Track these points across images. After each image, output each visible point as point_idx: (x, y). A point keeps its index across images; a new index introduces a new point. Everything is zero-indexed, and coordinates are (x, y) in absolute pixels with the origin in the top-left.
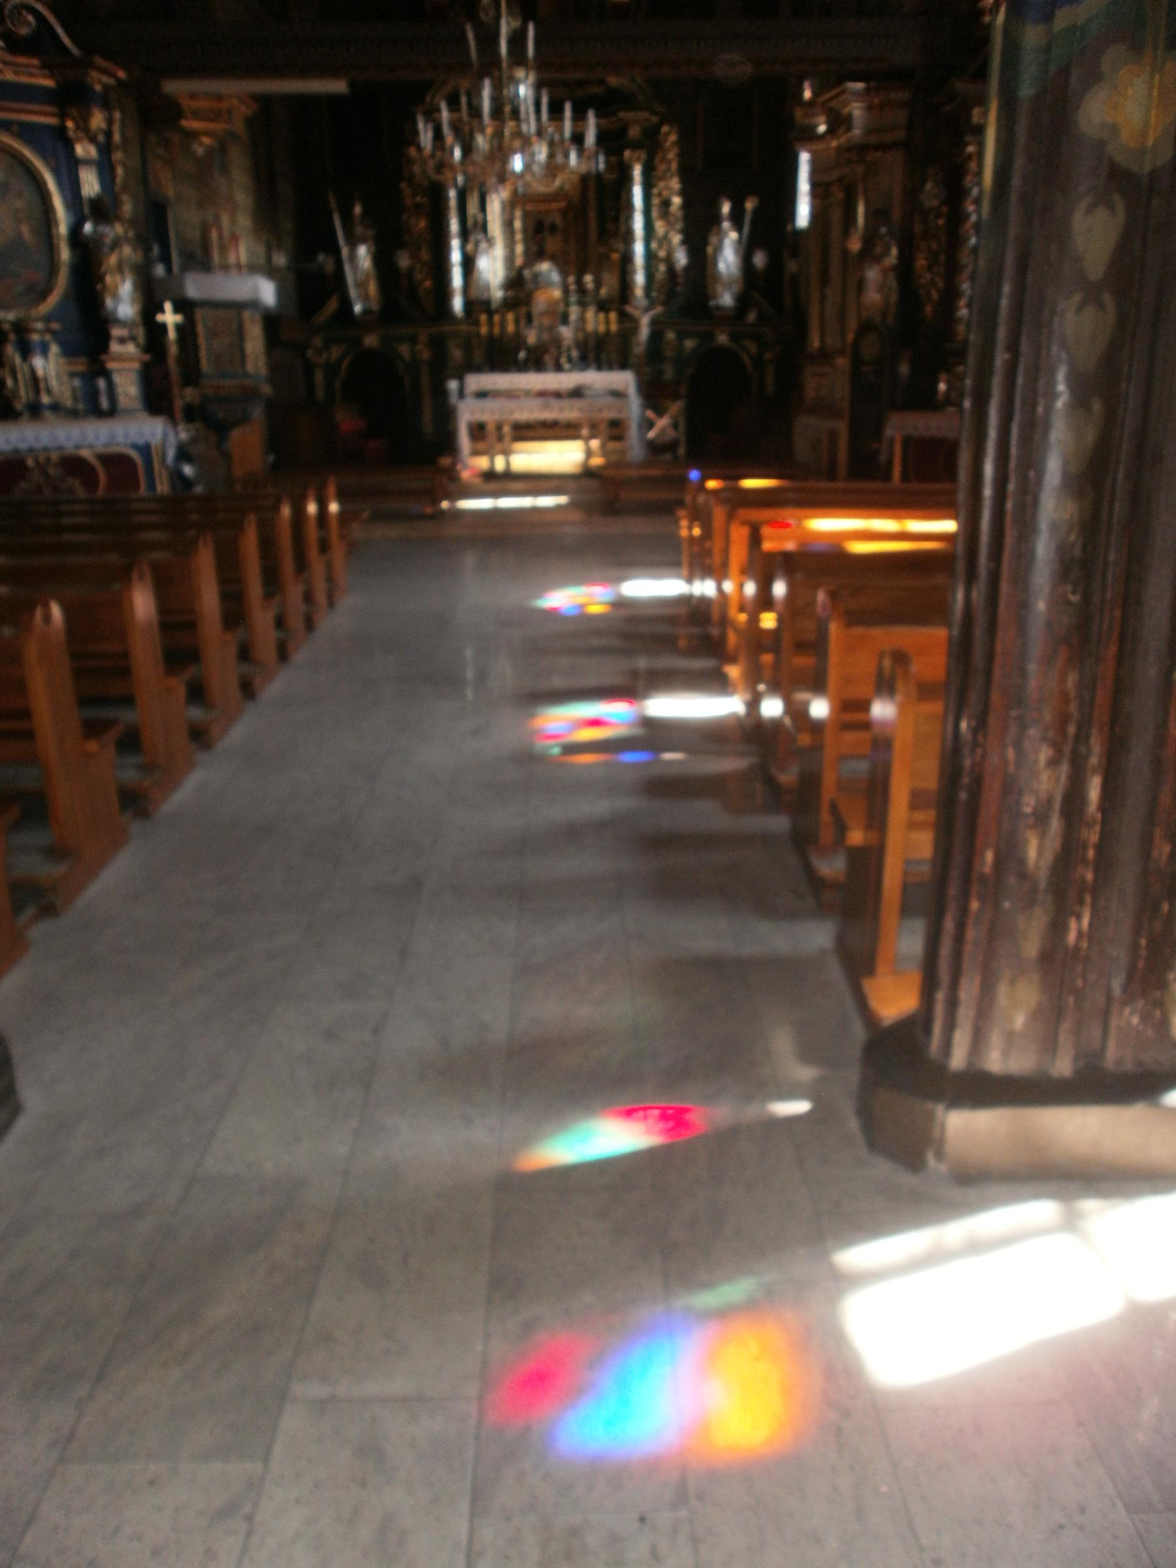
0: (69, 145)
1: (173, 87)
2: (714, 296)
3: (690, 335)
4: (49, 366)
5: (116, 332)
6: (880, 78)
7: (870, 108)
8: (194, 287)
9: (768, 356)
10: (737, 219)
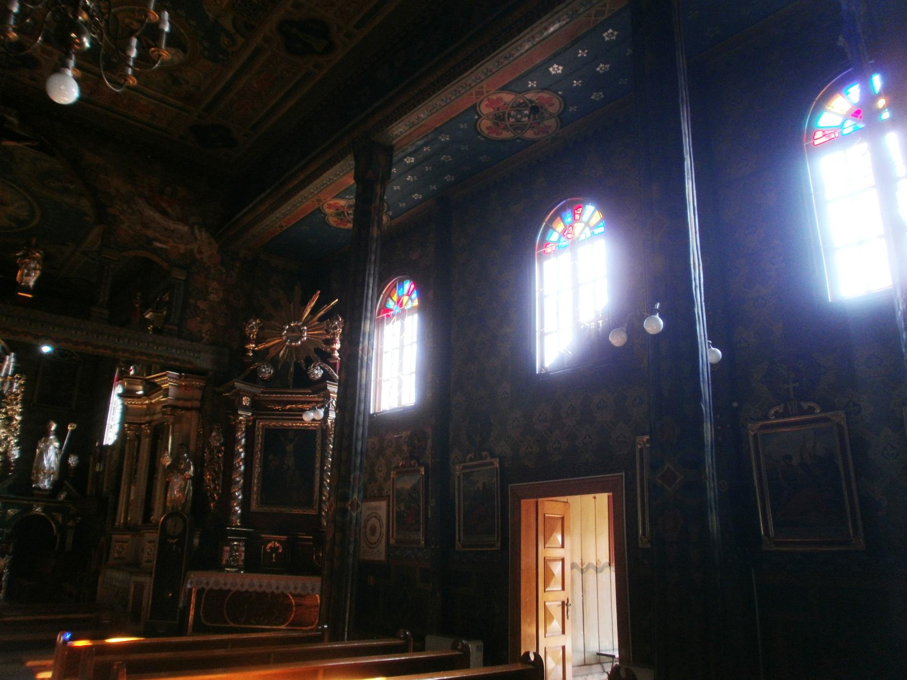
2: (37, 481)
3: (12, 506)
6: (186, 371)
7: (179, 387)
9: (70, 524)
10: (60, 435)
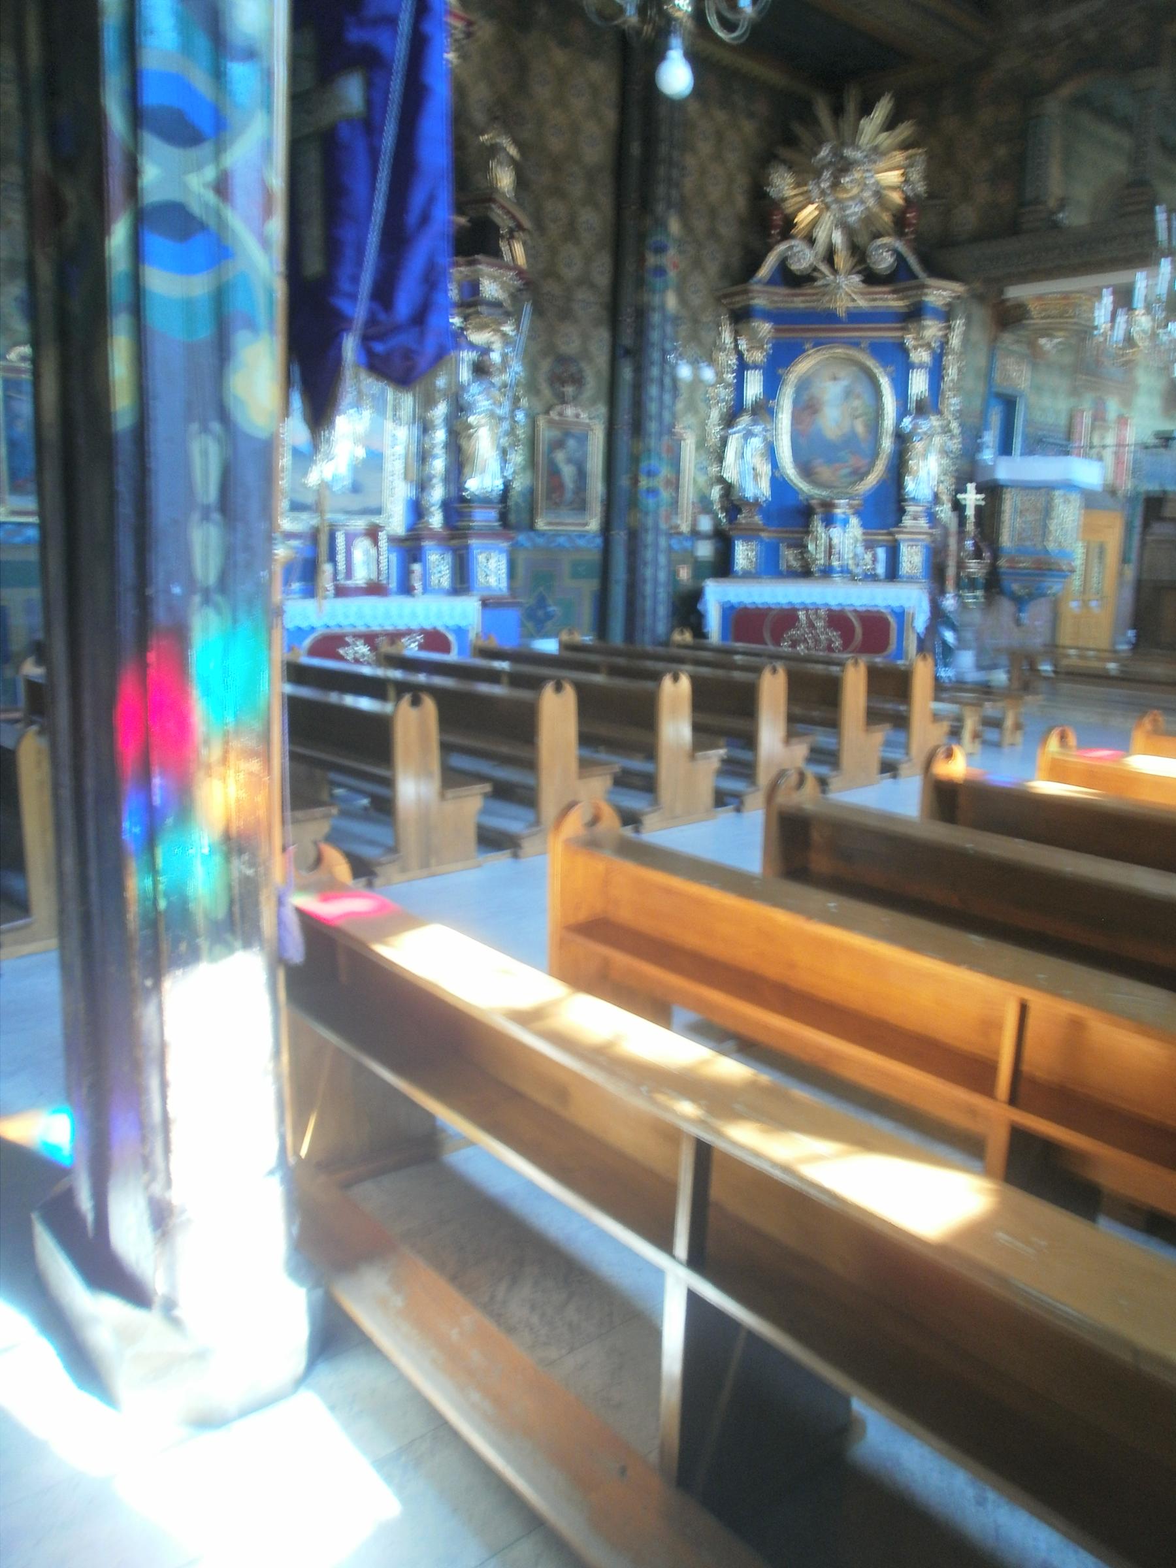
0: (905, 352)
1: (1016, 292)
4: (846, 538)
5: (911, 509)
8: (1005, 470)
